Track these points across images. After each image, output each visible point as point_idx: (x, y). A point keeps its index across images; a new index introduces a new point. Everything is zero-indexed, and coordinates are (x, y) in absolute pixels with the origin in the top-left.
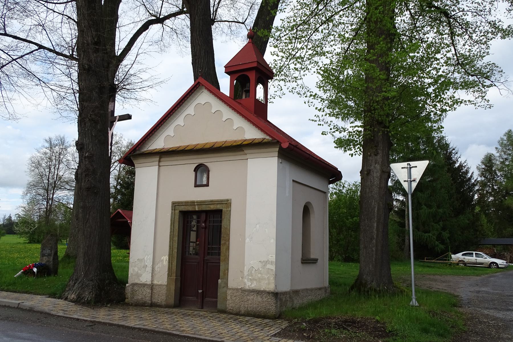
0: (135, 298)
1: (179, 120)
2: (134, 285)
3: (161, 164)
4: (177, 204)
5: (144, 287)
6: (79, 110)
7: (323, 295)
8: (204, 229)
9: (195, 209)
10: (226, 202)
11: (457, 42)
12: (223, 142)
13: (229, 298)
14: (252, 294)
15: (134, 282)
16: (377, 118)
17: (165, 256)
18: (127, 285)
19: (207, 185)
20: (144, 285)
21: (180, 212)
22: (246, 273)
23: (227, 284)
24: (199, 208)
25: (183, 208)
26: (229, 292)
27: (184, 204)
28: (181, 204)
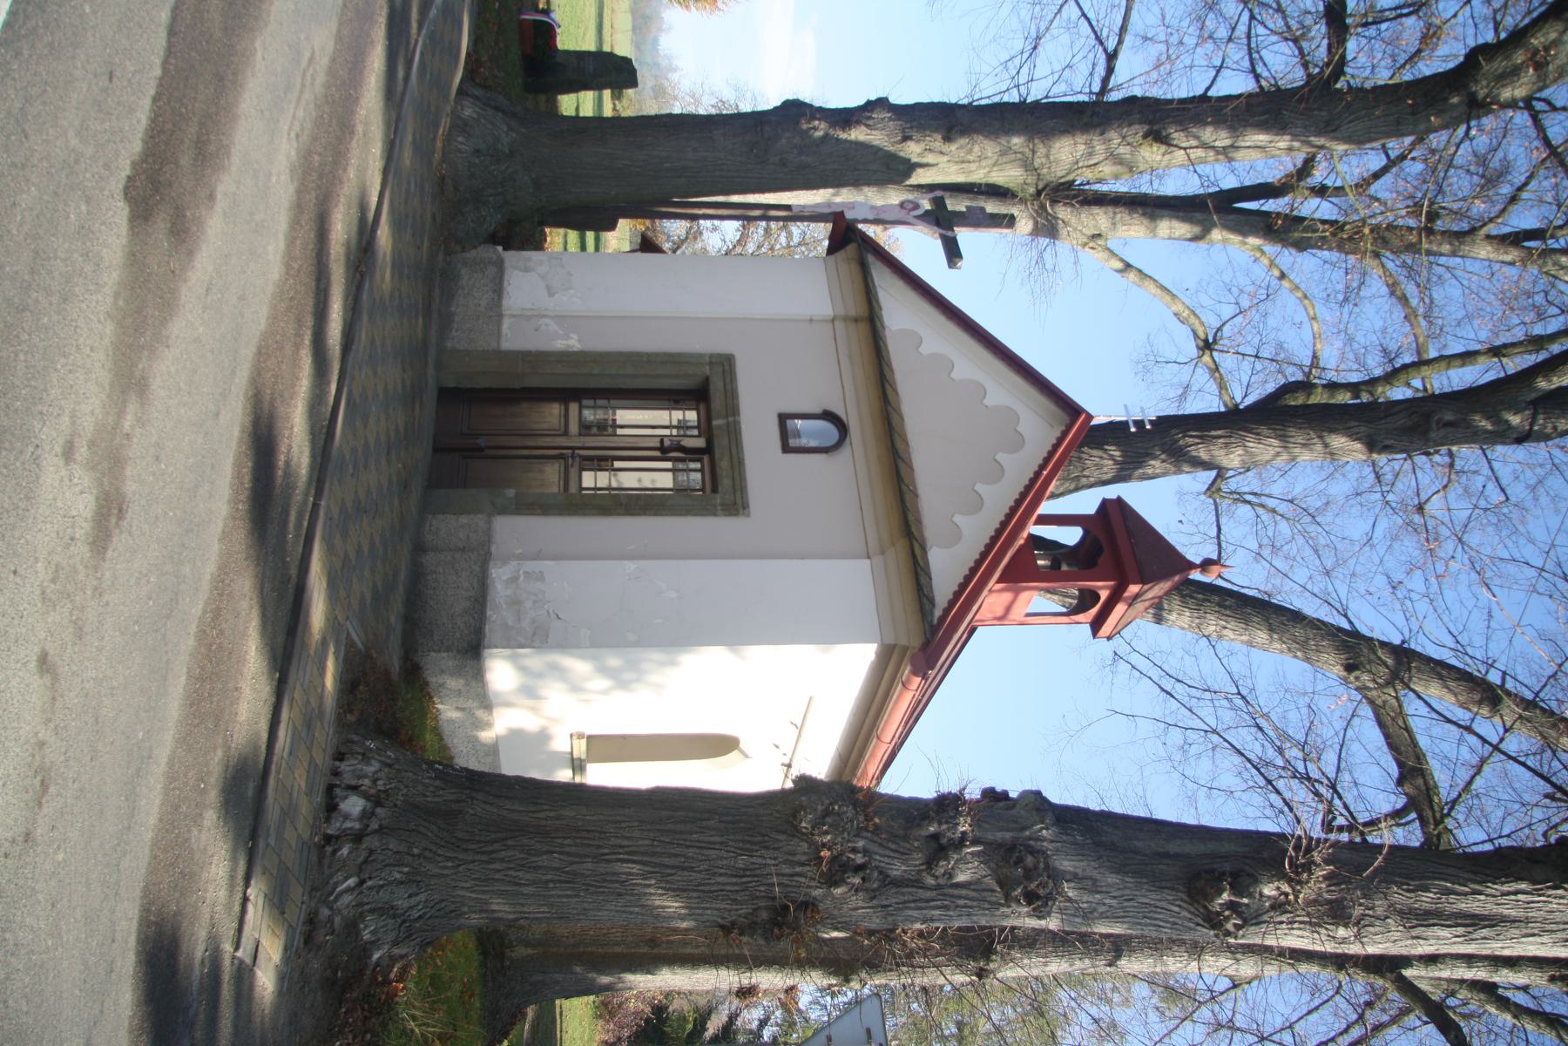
0: (463, 272)
1: (970, 363)
2: (500, 265)
3: (839, 325)
4: (727, 367)
5: (495, 291)
6: (970, 104)
7: (434, 522)
8: (658, 445)
9: (718, 418)
10: (739, 501)
11: (1488, 309)
12: (915, 487)
13: (464, 519)
14: (476, 585)
15: (507, 264)
16: (1083, 147)
17: (579, 341)
18: (500, 248)
19: (786, 449)
20: (498, 291)
21: (707, 380)
22: (530, 566)
23: (504, 511)
24: (719, 427)
25: (716, 387)
26: (480, 520)
27: (729, 387)
28: (728, 381)
